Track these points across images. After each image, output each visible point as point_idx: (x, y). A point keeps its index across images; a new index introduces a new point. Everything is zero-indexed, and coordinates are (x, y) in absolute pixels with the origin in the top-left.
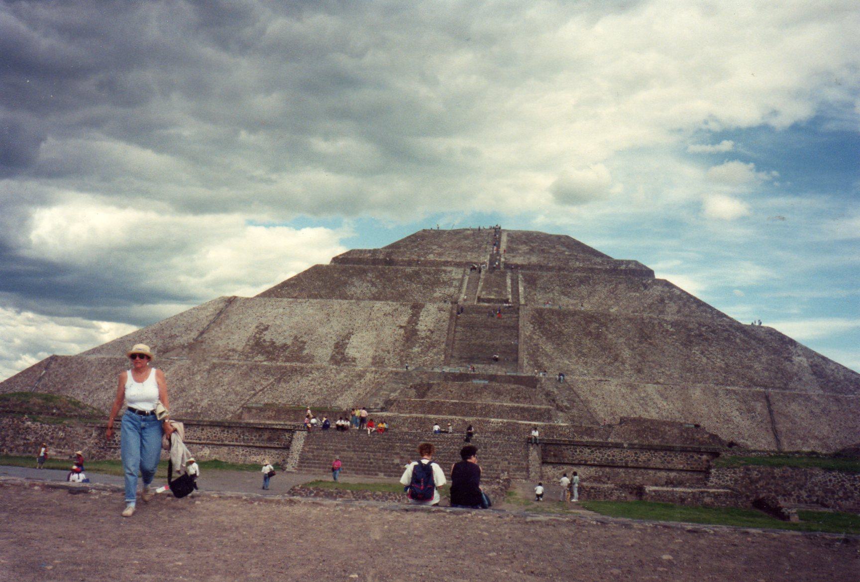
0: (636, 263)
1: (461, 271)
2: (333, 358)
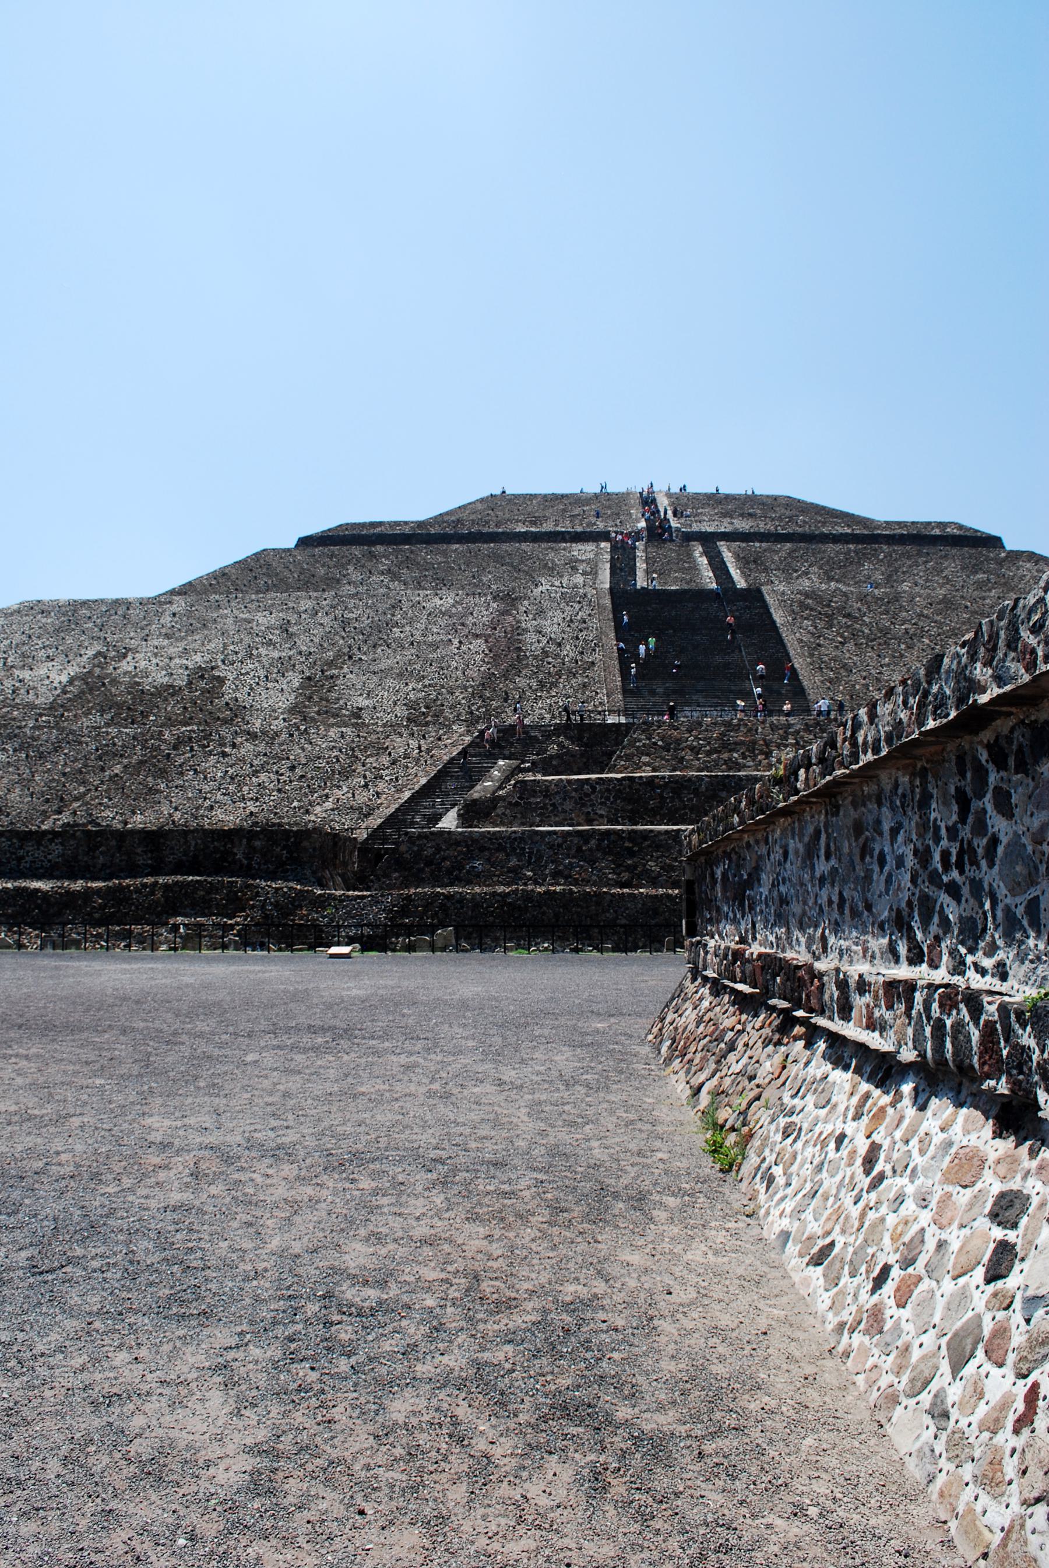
0: (961, 527)
1: (590, 547)
2: (293, 710)
